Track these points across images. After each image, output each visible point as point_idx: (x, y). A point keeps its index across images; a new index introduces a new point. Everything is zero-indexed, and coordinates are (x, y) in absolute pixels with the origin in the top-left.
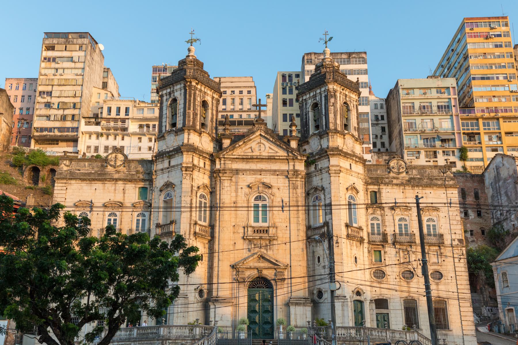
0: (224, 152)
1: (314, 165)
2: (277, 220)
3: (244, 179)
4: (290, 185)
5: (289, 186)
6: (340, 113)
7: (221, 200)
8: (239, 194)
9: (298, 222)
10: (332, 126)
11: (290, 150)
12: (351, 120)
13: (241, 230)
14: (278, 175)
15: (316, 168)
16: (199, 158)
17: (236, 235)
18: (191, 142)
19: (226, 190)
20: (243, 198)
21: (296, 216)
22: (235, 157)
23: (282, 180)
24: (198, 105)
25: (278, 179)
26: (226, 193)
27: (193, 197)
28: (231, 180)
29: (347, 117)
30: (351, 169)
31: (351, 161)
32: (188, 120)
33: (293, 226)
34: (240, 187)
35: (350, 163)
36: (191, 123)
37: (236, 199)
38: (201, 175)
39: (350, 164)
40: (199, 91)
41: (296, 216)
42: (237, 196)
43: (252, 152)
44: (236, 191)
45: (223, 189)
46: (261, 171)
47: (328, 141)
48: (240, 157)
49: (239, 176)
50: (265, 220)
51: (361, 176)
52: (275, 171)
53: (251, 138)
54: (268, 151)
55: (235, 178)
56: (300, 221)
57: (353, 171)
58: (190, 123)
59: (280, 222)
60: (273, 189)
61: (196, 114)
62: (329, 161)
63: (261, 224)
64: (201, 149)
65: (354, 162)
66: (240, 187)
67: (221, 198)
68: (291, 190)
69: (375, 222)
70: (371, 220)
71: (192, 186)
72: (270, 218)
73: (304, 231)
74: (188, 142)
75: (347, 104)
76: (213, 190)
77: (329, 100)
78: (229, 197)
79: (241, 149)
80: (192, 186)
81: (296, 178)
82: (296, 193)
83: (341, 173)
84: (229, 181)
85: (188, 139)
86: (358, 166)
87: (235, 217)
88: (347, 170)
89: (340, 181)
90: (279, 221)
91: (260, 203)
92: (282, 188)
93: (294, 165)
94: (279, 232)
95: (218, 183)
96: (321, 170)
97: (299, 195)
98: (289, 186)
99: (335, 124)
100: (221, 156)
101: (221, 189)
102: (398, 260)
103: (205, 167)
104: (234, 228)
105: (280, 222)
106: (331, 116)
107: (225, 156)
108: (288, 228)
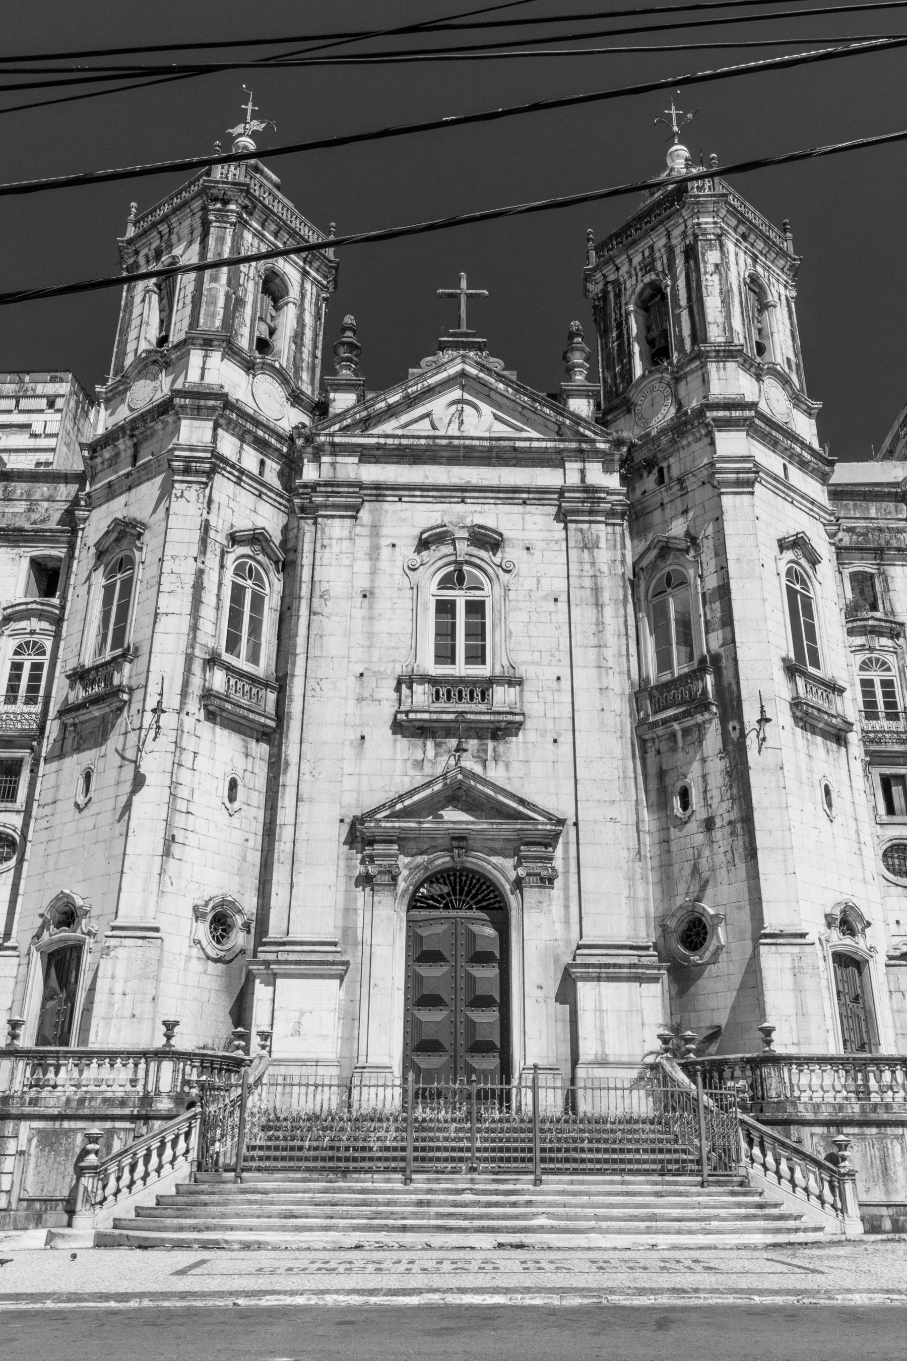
0: (334, 424)
1: (655, 471)
3: (403, 515)
4: (571, 534)
5: (567, 540)
6: (741, 302)
7: (317, 585)
8: (383, 565)
9: (604, 663)
10: (715, 334)
11: (568, 422)
13: (387, 692)
14: (524, 503)
16: (242, 440)
17: (369, 709)
18: (211, 379)
19: (336, 549)
21: (593, 641)
22: (373, 441)
23: (539, 519)
24: (247, 275)
25: (526, 517)
26: (334, 562)
27: (208, 563)
28: (355, 518)
32: (207, 312)
33: (585, 677)
34: (390, 541)
36: (218, 323)
37: (372, 581)
38: (246, 498)
40: (254, 235)
41: (593, 641)
42: (374, 572)
43: (434, 427)
44: (374, 554)
45: (324, 546)
46: (462, 492)
47: (705, 381)
48: (390, 441)
49: (386, 506)
50: (477, 656)
52: (515, 490)
53: (431, 381)
54: (491, 426)
55: (371, 511)
56: (610, 659)
58: (214, 323)
59: (533, 663)
60: (507, 550)
61: (240, 302)
62: (712, 443)
63: (461, 668)
64: (251, 412)
66: (384, 542)
67: (316, 578)
68: (573, 553)
69: (876, 676)
70: (861, 669)
71: (206, 527)
72: (498, 650)
73: (623, 694)
74: (202, 377)
75: (761, 287)
76: (291, 556)
77: (703, 255)
80: (206, 527)
82: (593, 564)
84: (348, 522)
85: (203, 369)
87: (367, 643)
89: (758, 512)
91: (460, 598)
92: (539, 546)
93: (583, 472)
94: (528, 696)
95: (307, 528)
96: (680, 481)
97: (605, 568)
98: (567, 540)
99: (728, 328)
100: (323, 439)
101: (318, 549)
103: (261, 473)
104: (362, 684)
105: (533, 663)
106: (713, 304)
107: (337, 440)
108: (566, 683)
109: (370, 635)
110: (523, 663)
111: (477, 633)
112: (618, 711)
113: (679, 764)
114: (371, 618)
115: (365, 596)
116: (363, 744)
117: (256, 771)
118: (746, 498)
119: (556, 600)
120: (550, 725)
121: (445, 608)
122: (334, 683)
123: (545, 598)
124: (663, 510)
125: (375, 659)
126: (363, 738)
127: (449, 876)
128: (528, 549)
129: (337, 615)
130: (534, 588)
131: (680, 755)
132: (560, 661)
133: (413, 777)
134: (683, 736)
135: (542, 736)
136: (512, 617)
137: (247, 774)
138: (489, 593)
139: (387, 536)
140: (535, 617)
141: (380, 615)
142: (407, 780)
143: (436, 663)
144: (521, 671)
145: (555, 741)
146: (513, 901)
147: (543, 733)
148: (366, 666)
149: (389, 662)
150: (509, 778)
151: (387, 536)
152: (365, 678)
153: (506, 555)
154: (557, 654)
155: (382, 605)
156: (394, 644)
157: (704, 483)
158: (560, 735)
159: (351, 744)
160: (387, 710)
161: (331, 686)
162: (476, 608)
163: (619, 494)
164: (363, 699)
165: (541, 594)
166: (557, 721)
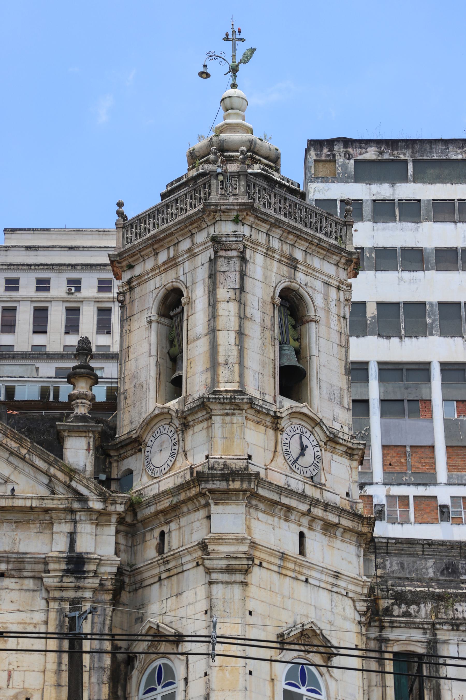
12: (314, 359)
15: (160, 549)
29: (296, 344)
30: (302, 552)
31: (305, 521)
35: (297, 530)
39: (302, 535)
47: (210, 439)
51: (351, 587)
57: (311, 566)
65: (318, 525)
81: (77, 588)
83: (256, 570)
86: (338, 543)
88: (283, 556)
89: (251, 605)
93: (72, 537)
118: (237, 590)
124: (161, 585)
157: (198, 565)
163: (111, 565)
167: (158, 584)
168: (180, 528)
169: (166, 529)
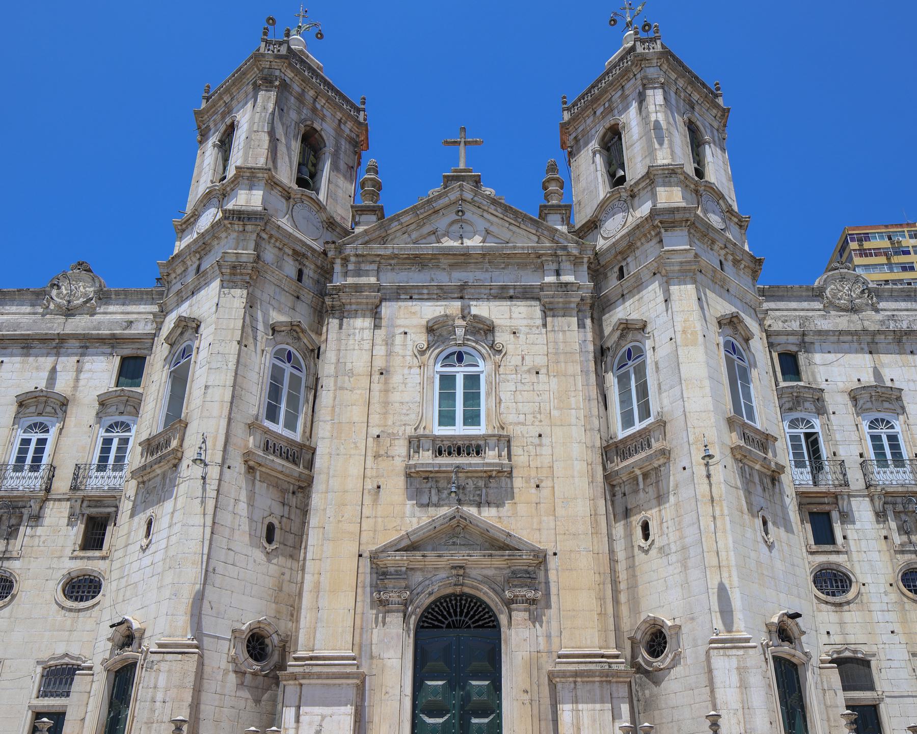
2: (511, 418)
8: (398, 349)
20: (408, 358)
26: (357, 347)
42: (389, 354)
50: (472, 418)
63: (459, 429)
73: (594, 446)
78: (366, 357)
79: (406, 235)
90: (516, 420)
91: (460, 372)
102: (886, 538)
109: (386, 404)
110: (511, 424)
111: (472, 398)
112: (589, 461)
113: (641, 502)
114: (386, 391)
115: (382, 374)
116: (379, 492)
117: (293, 517)
119: (537, 373)
120: (533, 473)
121: (447, 381)
122: (355, 443)
123: (529, 371)
125: (390, 422)
126: (379, 487)
127: (451, 600)
128: (514, 333)
129: (358, 388)
130: (520, 363)
131: (642, 494)
132: (541, 421)
133: (419, 518)
134: (644, 479)
135: (527, 482)
136: (503, 386)
137: (284, 520)
138: (483, 368)
139: (400, 326)
140: (520, 387)
141: (394, 388)
142: (415, 520)
143: (440, 425)
144: (510, 430)
145: (538, 486)
146: (503, 619)
147: (528, 480)
148: (382, 429)
149: (400, 426)
150: (500, 518)
151: (400, 326)
152: (381, 439)
153: (496, 338)
154: (538, 416)
155: (396, 379)
156: (405, 411)
158: (542, 481)
159: (369, 492)
160: (399, 464)
161: (353, 446)
162: (472, 381)
164: (379, 456)
165: (525, 368)
166: (539, 469)
167: (621, 299)
168: (636, 258)
169: (624, 264)
